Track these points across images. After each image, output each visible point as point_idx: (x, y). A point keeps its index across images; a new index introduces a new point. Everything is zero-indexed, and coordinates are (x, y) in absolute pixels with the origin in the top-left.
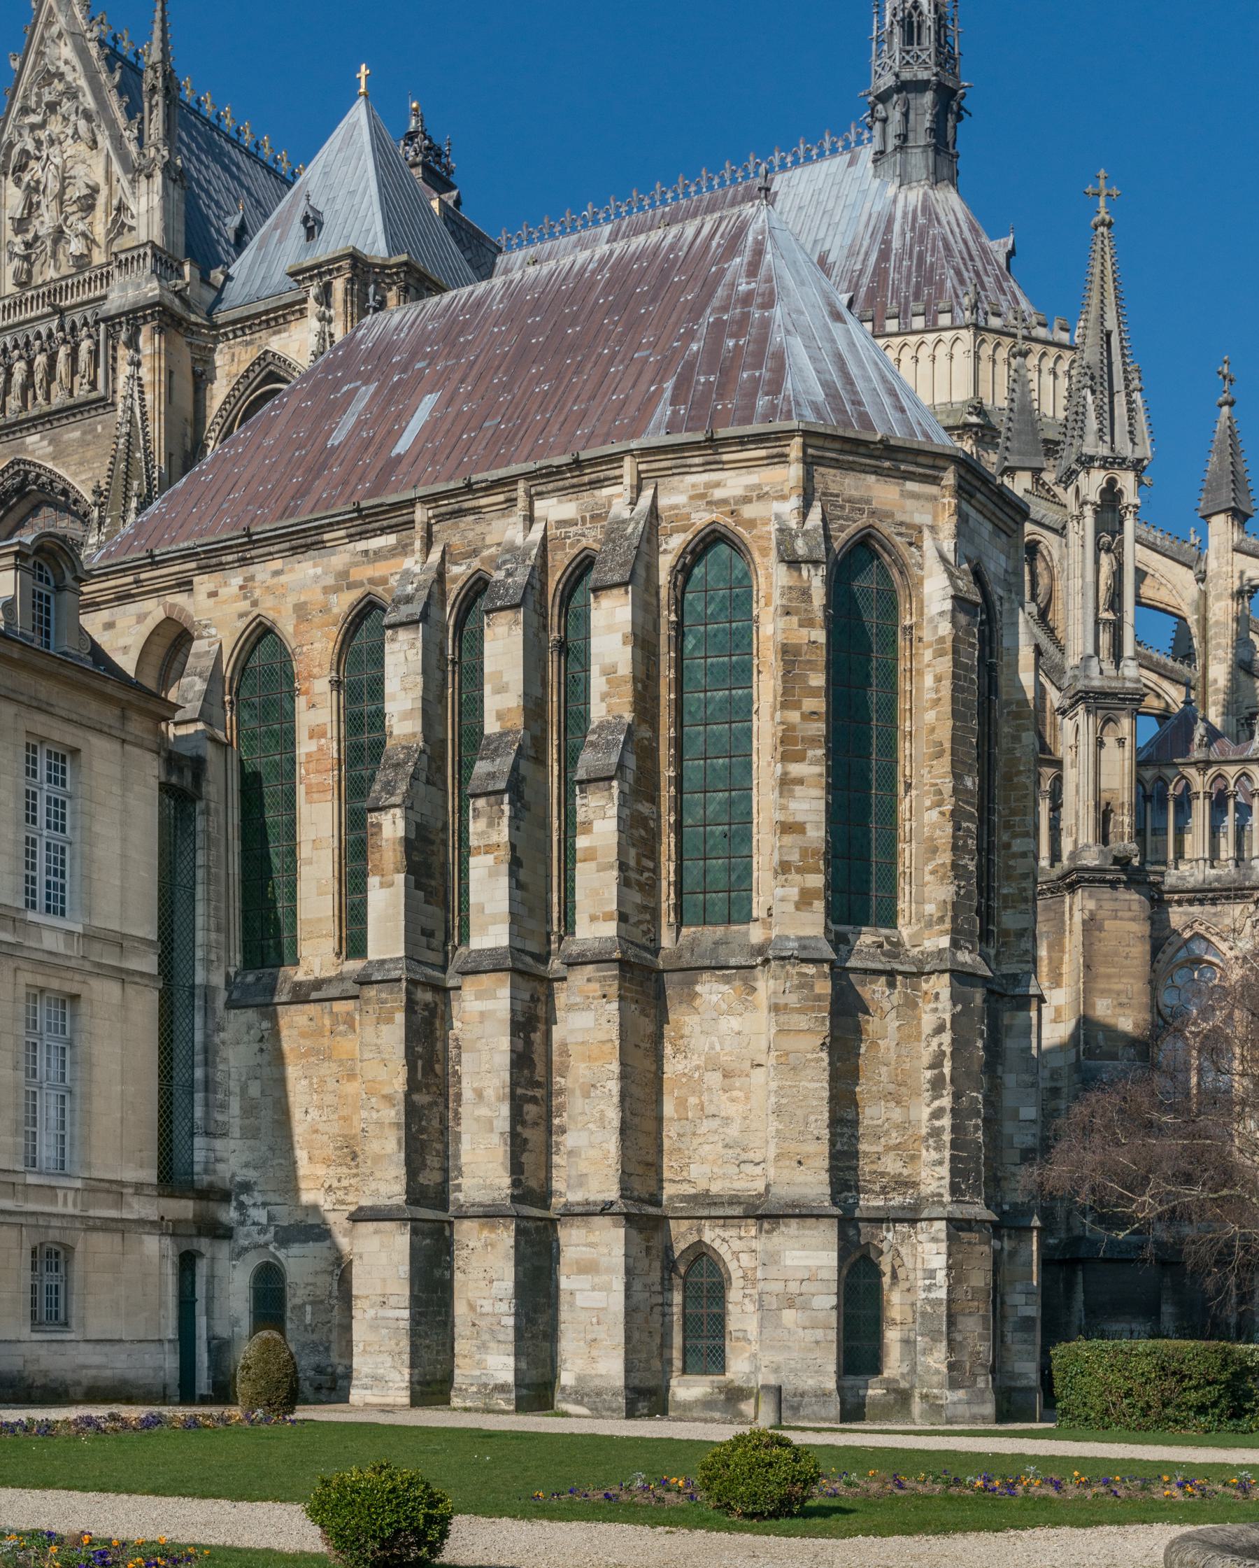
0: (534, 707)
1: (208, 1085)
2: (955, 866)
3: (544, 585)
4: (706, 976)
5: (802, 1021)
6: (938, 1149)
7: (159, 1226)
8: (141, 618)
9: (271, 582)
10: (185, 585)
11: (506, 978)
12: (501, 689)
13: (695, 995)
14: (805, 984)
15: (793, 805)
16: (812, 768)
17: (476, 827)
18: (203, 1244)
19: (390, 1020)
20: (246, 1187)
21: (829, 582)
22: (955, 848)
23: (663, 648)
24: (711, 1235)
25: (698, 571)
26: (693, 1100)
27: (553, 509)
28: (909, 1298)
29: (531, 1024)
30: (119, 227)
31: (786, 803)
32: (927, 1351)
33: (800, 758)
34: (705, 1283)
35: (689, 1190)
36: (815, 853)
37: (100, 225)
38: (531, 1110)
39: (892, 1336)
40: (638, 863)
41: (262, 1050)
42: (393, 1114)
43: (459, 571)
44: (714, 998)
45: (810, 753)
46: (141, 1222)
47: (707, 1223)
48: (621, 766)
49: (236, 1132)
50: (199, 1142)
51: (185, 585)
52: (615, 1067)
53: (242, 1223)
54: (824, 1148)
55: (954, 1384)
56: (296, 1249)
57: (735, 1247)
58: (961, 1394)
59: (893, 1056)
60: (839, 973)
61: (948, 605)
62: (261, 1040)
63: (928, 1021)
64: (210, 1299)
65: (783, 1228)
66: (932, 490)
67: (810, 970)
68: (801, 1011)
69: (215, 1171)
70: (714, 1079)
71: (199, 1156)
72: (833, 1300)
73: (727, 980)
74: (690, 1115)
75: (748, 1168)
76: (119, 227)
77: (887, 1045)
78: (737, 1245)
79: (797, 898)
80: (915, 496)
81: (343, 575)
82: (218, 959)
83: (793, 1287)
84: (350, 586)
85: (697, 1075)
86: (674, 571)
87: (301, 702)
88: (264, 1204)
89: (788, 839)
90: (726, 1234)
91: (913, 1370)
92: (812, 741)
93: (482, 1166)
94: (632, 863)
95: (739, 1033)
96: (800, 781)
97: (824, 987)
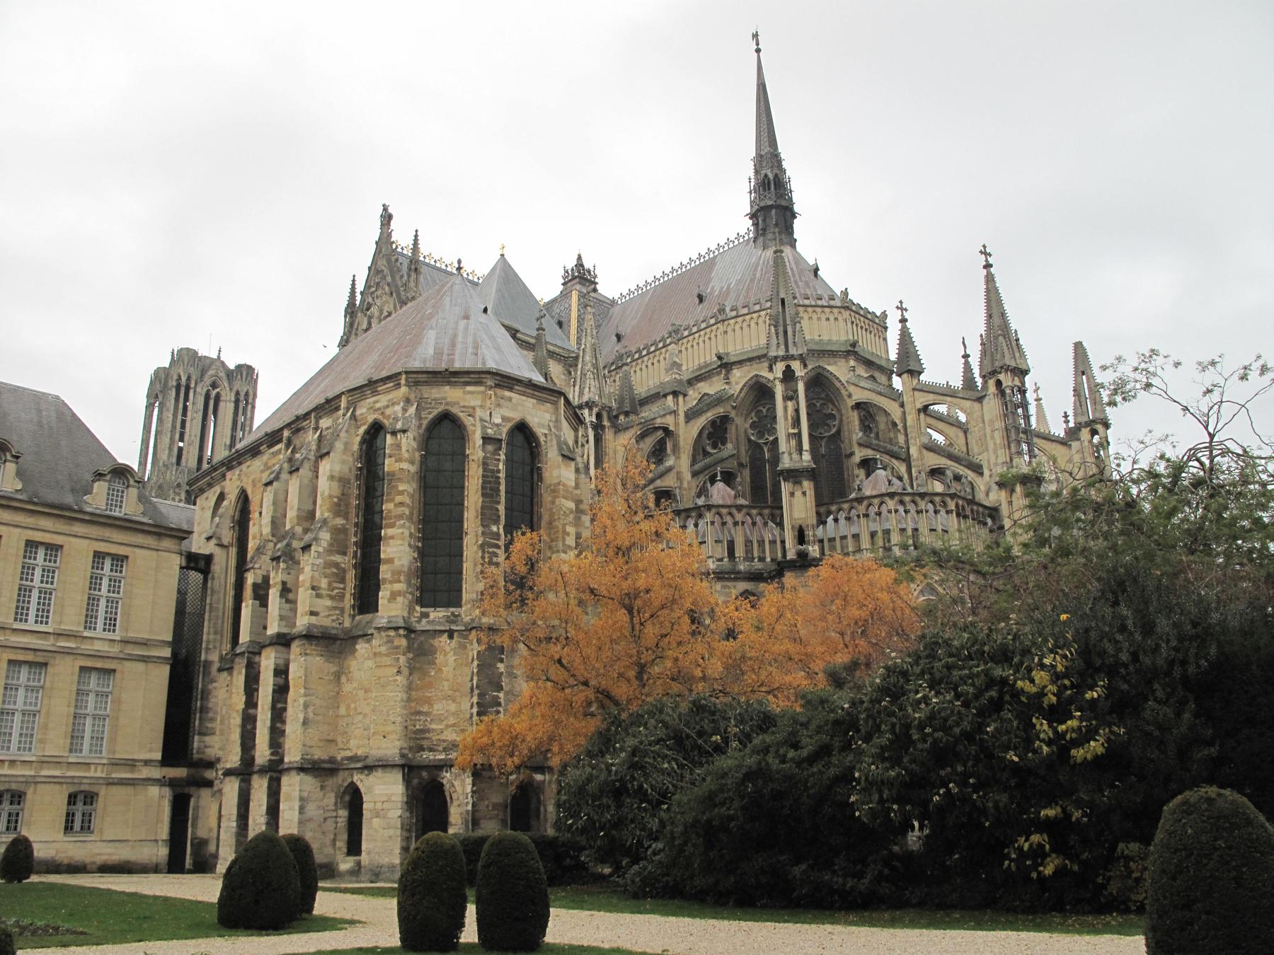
1: (204, 710)
7: (161, 782)
13: (356, 650)
18: (192, 790)
20: (218, 760)
24: (357, 778)
31: (398, 549)
34: (354, 801)
35: (349, 754)
36: (399, 573)
40: (330, 584)
46: (148, 779)
50: (196, 738)
54: (399, 728)
57: (364, 782)
59: (451, 676)
64: (195, 819)
68: (387, 655)
70: (361, 693)
71: (196, 745)
77: (448, 671)
81: (266, 464)
83: (379, 806)
84: (269, 468)
86: (363, 441)
92: (400, 517)
96: (392, 538)
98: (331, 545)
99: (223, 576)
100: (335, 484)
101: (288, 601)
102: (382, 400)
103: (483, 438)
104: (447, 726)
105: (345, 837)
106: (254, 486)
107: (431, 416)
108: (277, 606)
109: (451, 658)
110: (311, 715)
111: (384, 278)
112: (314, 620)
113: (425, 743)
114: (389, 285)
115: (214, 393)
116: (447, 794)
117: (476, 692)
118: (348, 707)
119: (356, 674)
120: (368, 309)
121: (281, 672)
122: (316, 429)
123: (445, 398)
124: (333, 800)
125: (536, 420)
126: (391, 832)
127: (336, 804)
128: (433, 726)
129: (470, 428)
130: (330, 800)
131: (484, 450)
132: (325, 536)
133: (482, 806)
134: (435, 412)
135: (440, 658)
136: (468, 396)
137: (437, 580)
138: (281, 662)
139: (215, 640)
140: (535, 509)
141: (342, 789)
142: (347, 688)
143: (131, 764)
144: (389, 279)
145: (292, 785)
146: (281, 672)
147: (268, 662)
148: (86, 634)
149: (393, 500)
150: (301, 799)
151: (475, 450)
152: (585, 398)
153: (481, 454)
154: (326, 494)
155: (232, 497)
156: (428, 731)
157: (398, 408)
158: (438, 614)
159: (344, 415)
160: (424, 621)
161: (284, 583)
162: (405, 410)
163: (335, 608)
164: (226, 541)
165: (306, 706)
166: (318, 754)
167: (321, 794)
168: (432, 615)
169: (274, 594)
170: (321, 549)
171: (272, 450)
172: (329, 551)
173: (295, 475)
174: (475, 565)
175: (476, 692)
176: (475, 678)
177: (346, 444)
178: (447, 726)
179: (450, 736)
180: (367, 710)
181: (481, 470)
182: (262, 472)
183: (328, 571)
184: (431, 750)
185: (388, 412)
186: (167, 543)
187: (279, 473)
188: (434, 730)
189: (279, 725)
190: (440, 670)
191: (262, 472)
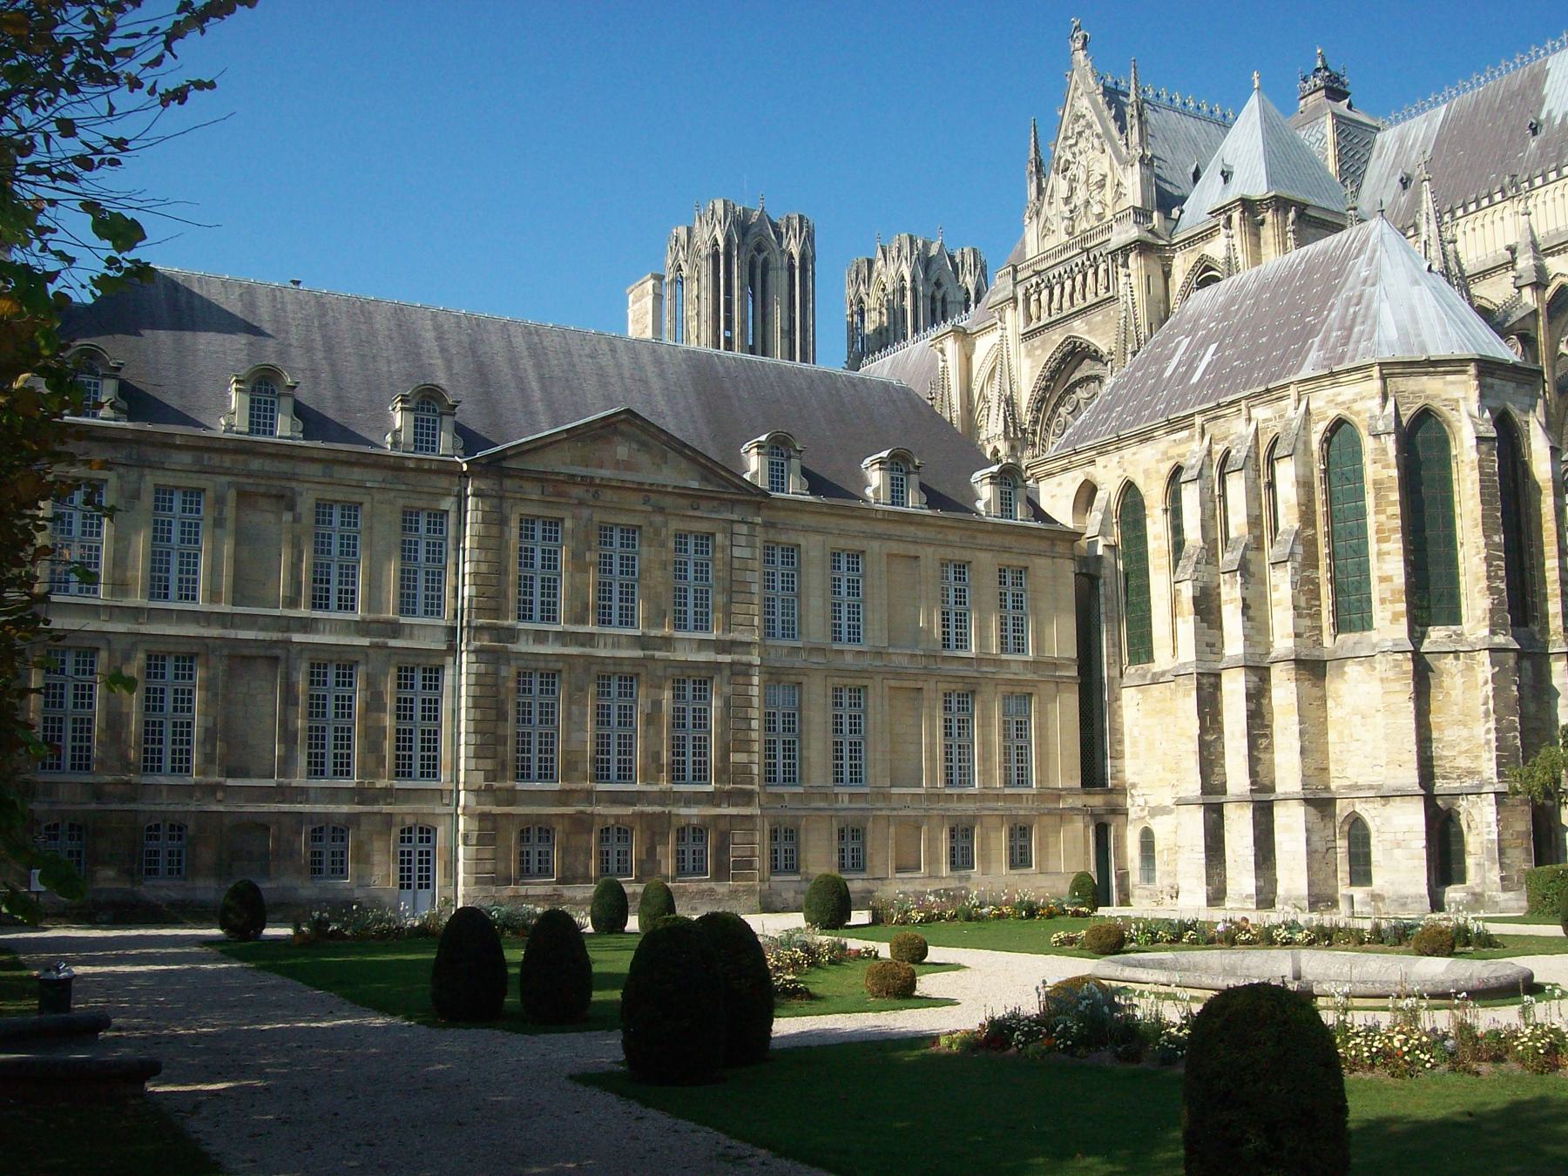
0: (1254, 522)
2: (1489, 588)
3: (1257, 455)
5: (1397, 686)
10: (1092, 462)
11: (1242, 671)
14: (1397, 664)
15: (1385, 566)
16: (1395, 546)
17: (1224, 590)
20: (1134, 786)
21: (1398, 441)
22: (1489, 578)
23: (1317, 483)
24: (1360, 808)
25: (1335, 439)
26: (1346, 732)
27: (1260, 413)
28: (1479, 839)
29: (1257, 698)
30: (1119, 196)
31: (1387, 565)
32: (1490, 870)
33: (1387, 540)
37: (1109, 194)
38: (1263, 742)
39: (1470, 861)
43: (1219, 449)
46: (1072, 809)
48: (1292, 554)
49: (1127, 755)
51: (1092, 462)
52: (1296, 718)
55: (1505, 889)
56: (1158, 818)
57: (1371, 814)
58: (1511, 894)
59: (1460, 698)
61: (1474, 442)
63: (1481, 679)
66: (1464, 377)
67: (1400, 657)
70: (1357, 719)
72: (1424, 843)
73: (1361, 663)
75: (1378, 769)
76: (1119, 196)
78: (1373, 813)
80: (1453, 383)
81: (1165, 453)
83: (1400, 837)
89: (1384, 585)
90: (1368, 806)
91: (1483, 882)
92: (1394, 530)
93: (1237, 776)
94: (1303, 604)
97: (1409, 666)
98: (1304, 559)
104: (1461, 753)
107: (1411, 412)
109: (1459, 680)
114: (1098, 136)
115: (760, 259)
126: (1416, 862)
128: (1445, 753)
133: (1507, 836)
134: (1415, 408)
135: (1447, 681)
136: (1450, 388)
140: (1522, 510)
143: (1058, 795)
144: (1098, 129)
148: (1004, 657)
153: (1474, 456)
155: (1109, 491)
163: (1314, 628)
165: (1301, 733)
166: (1315, 783)
171: (1173, 437)
178: (1461, 753)
179: (1463, 763)
182: (1162, 461)
184: (1444, 778)
186: (1061, 548)
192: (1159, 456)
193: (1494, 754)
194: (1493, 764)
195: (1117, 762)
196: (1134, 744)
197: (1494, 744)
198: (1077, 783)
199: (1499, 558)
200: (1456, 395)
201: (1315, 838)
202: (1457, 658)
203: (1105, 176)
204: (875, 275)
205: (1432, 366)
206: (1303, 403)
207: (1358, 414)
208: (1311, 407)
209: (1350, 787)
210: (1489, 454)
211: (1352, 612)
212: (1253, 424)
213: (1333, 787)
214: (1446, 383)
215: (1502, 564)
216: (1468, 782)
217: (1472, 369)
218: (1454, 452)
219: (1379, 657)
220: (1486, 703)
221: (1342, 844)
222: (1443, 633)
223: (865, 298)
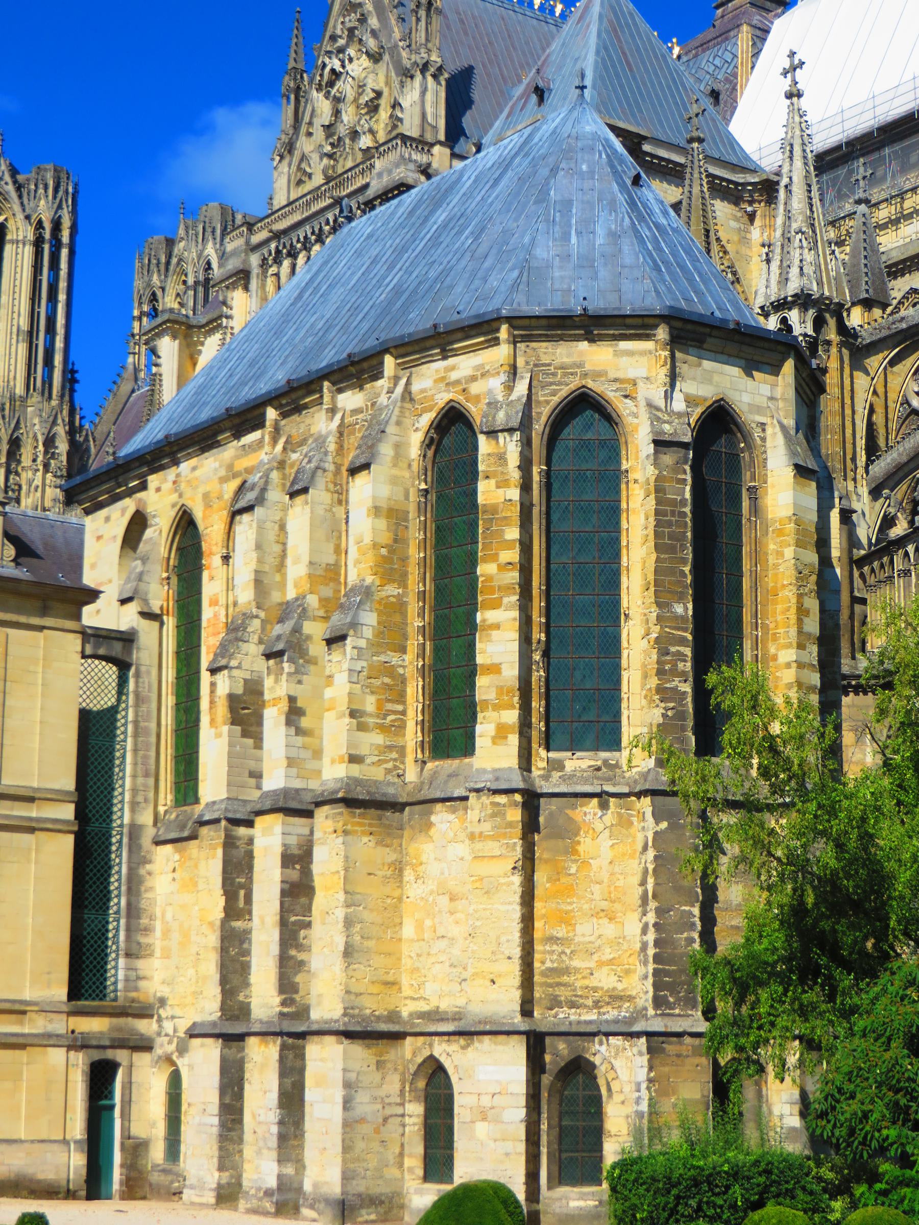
4: (439, 806)
5: (493, 847)
6: (645, 963)
8: (123, 511)
9: (191, 476)
12: (297, 561)
13: (430, 825)
14: (498, 812)
18: (121, 1056)
19: (214, 857)
20: (162, 1002)
26: (428, 923)
35: (424, 1007)
40: (379, 708)
41: (174, 879)
42: (213, 939)
44: (444, 826)
45: (506, 600)
47: (437, 1038)
49: (158, 953)
50: (122, 962)
53: (159, 1034)
59: (605, 876)
60: (531, 801)
62: (174, 870)
64: (127, 1103)
65: (476, 1044)
67: (502, 799)
68: (492, 838)
69: (136, 989)
70: (444, 901)
74: (426, 936)
79: (493, 734)
82: (146, 800)
83: (486, 1101)
85: (431, 899)
87: (205, 575)
88: (173, 1017)
92: (508, 589)
95: (462, 859)
96: (497, 626)
97: (515, 815)
98: (379, 634)
99: (154, 672)
100: (382, 524)
101: (299, 732)
102: (463, 365)
103: (656, 443)
105: (420, 1149)
106: (208, 505)
107: (556, 399)
108: (282, 741)
110: (357, 938)
111: (363, 20)
112: (356, 770)
113: (563, 994)
114: (374, 33)
116: (601, 1082)
117: (652, 905)
118: (419, 926)
119: (433, 869)
120: (331, 84)
121: (298, 859)
122: (333, 411)
123: (580, 365)
124: (397, 1086)
125: (746, 398)
126: (509, 1146)
127: (402, 1091)
128: (576, 963)
129: (629, 420)
130: (393, 1085)
131: (656, 464)
132: (370, 619)
133: (666, 1105)
134: (564, 391)
135: (585, 844)
136: (624, 361)
137: (572, 698)
138: (293, 841)
139: (145, 785)
141: (412, 1068)
142: (414, 890)
145: (325, 1060)
146: (298, 859)
147: (269, 838)
149: (494, 558)
150: (347, 1085)
151: (639, 463)
152: (793, 287)
153: (651, 472)
154: (368, 540)
156: (567, 971)
157: (496, 384)
158: (578, 763)
159: (390, 391)
160: (556, 775)
161: (292, 699)
162: (509, 387)
163: (390, 748)
164: (155, 606)
165: (348, 923)
167: (377, 1077)
168: (570, 766)
169: (273, 719)
170: (362, 643)
172: (377, 646)
173: (299, 500)
174: (645, 676)
175: (652, 905)
176: (651, 881)
177: (397, 446)
178: (601, 964)
179: (606, 980)
180: (456, 931)
181: (652, 502)
182: (223, 480)
183: (377, 682)
184: (573, 1005)
185: (475, 388)
187: (264, 490)
188: (577, 970)
189: (293, 952)
190: (586, 863)
191: (223, 480)
192: (223, 473)
193: (651, 967)
194: (649, 983)
195: (140, 964)
196: (166, 933)
197: (651, 951)
198: (61, 992)
199: (682, 641)
200: (631, 374)
201: (362, 1098)
202: (604, 806)
203: (379, 94)
204: (174, 261)
205: (593, 325)
206: (403, 382)
207: (477, 399)
208: (415, 387)
209: (422, 1015)
210: (677, 467)
211: (450, 730)
212: (338, 416)
213: (405, 1014)
214: (617, 354)
215: (688, 651)
216: (611, 1014)
217: (662, 333)
218: (624, 467)
219: (472, 796)
220: (643, 883)
221: (415, 1110)
222: (585, 764)
223: (159, 293)
